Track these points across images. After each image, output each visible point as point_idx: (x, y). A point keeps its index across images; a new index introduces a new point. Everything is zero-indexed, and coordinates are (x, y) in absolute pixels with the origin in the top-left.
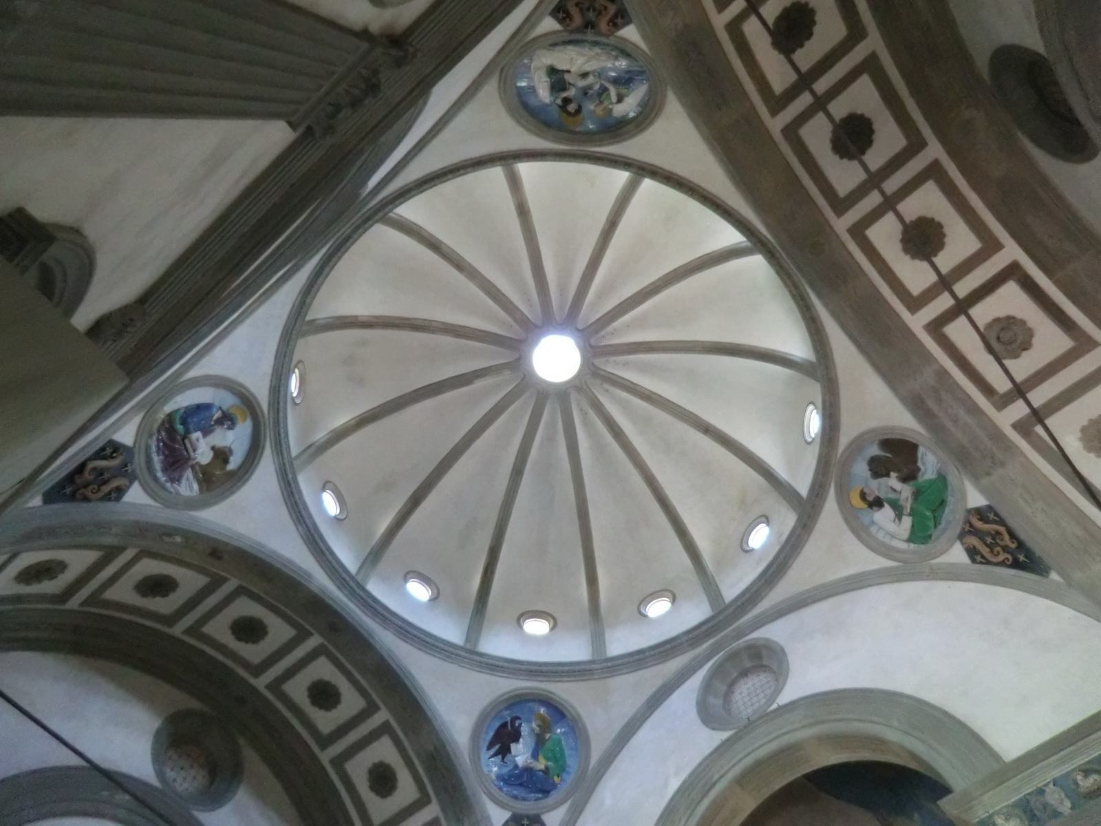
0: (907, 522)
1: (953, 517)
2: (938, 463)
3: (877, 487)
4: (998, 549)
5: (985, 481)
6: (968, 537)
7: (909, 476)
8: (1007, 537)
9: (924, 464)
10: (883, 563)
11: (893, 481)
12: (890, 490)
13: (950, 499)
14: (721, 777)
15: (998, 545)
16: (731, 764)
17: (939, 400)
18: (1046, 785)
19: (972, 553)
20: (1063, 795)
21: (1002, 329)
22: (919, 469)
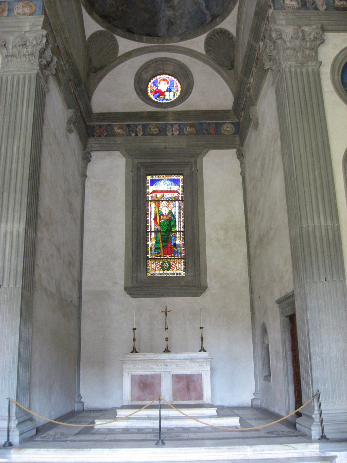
20: (324, 3)
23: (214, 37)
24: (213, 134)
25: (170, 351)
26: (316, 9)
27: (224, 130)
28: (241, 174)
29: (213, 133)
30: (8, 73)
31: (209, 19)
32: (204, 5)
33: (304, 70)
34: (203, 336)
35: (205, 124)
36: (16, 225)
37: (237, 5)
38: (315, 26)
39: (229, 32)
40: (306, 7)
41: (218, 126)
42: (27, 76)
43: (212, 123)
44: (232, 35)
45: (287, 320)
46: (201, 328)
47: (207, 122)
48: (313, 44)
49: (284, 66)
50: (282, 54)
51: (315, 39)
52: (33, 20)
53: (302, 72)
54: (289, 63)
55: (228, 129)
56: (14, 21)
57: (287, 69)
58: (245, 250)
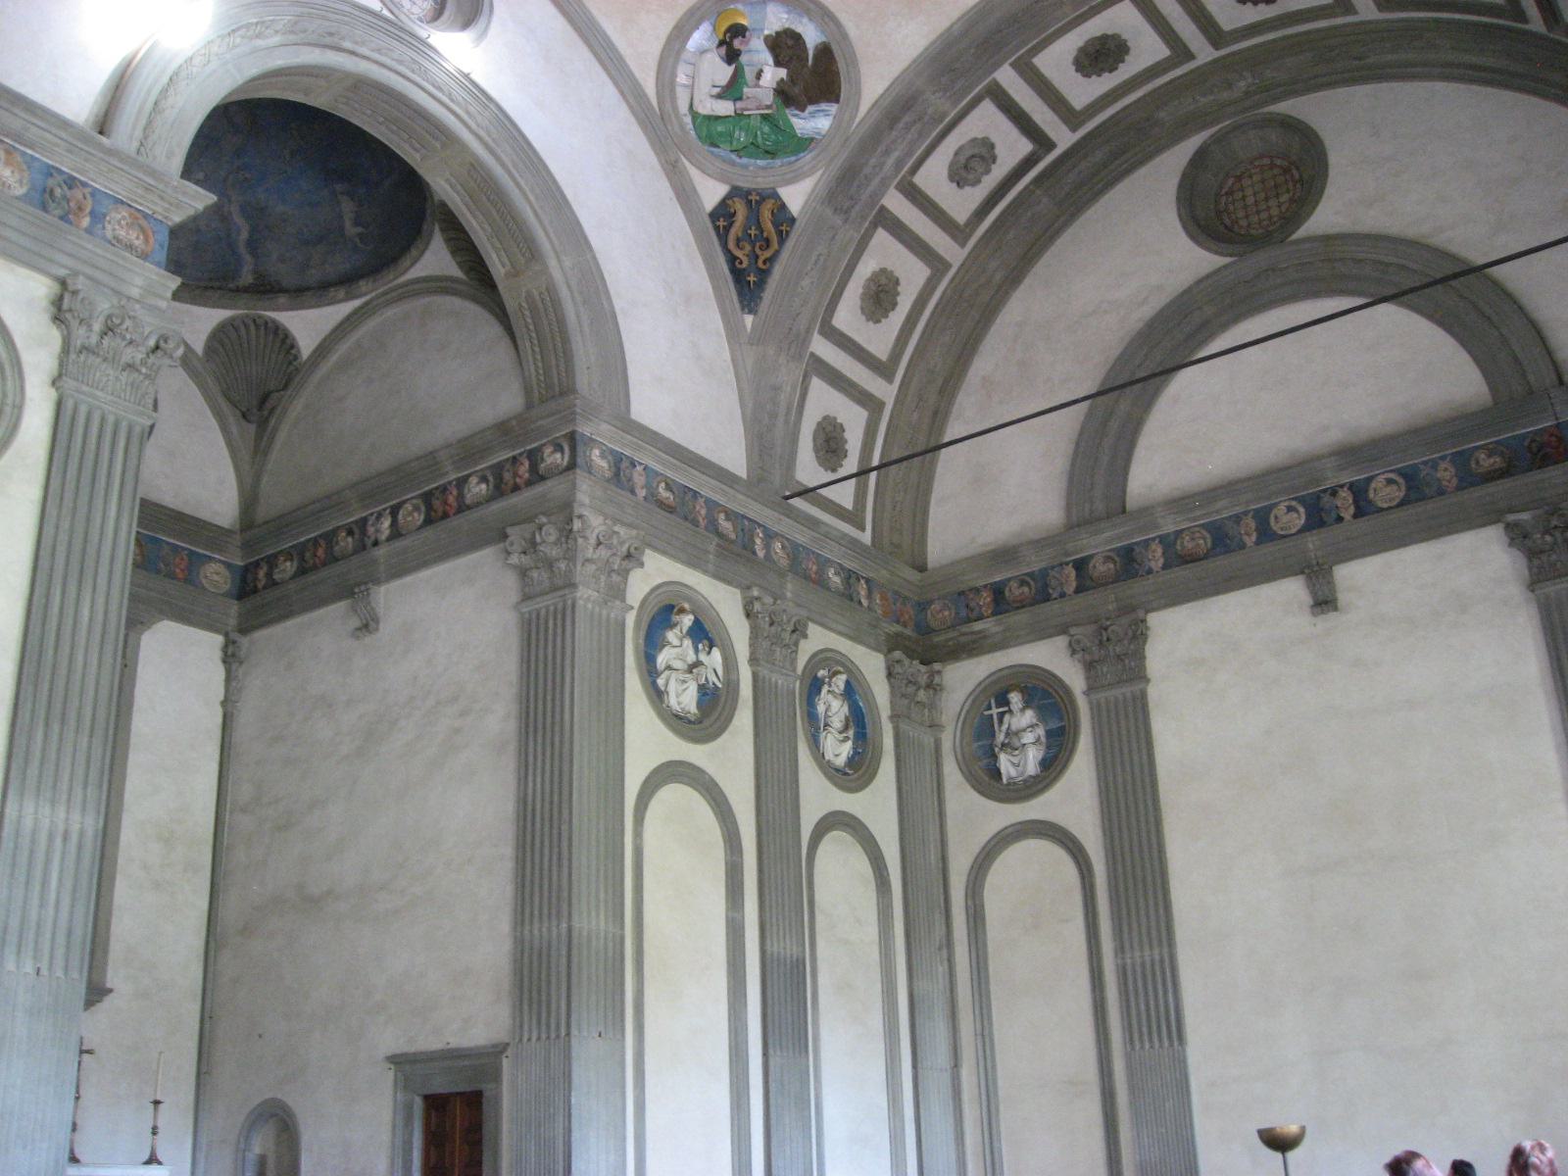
0: (725, 108)
1: (755, 173)
2: (818, 134)
3: (757, 53)
4: (748, 248)
5: (829, 212)
6: (743, 202)
7: (785, 95)
8: (767, 254)
9: (813, 115)
10: (650, 89)
11: (773, 75)
12: (756, 70)
13: (778, 162)
14: (353, 53)
15: (754, 247)
16: (375, 56)
17: (908, 128)
18: (641, 464)
19: (722, 215)
21: (982, 158)
22: (803, 110)
23: (243, 329)
24: (179, 580)
25: (78, 1156)
26: (633, 492)
27: (206, 577)
28: (224, 703)
29: (181, 576)
30: (82, 397)
31: (247, 278)
32: (244, 235)
33: (604, 612)
34: (79, 1122)
35: (164, 545)
36: (76, 817)
37: (357, 303)
38: (634, 532)
39: (294, 339)
40: (619, 481)
41: (196, 561)
42: (124, 423)
43: (184, 549)
44: (299, 351)
45: (418, 1104)
46: (157, 1103)
47: (171, 541)
48: (624, 563)
49: (578, 595)
50: (579, 568)
51: (628, 556)
52: (154, 277)
53: (600, 615)
54: (590, 592)
55: (216, 577)
56: (109, 256)
57: (581, 602)
58: (204, 904)
